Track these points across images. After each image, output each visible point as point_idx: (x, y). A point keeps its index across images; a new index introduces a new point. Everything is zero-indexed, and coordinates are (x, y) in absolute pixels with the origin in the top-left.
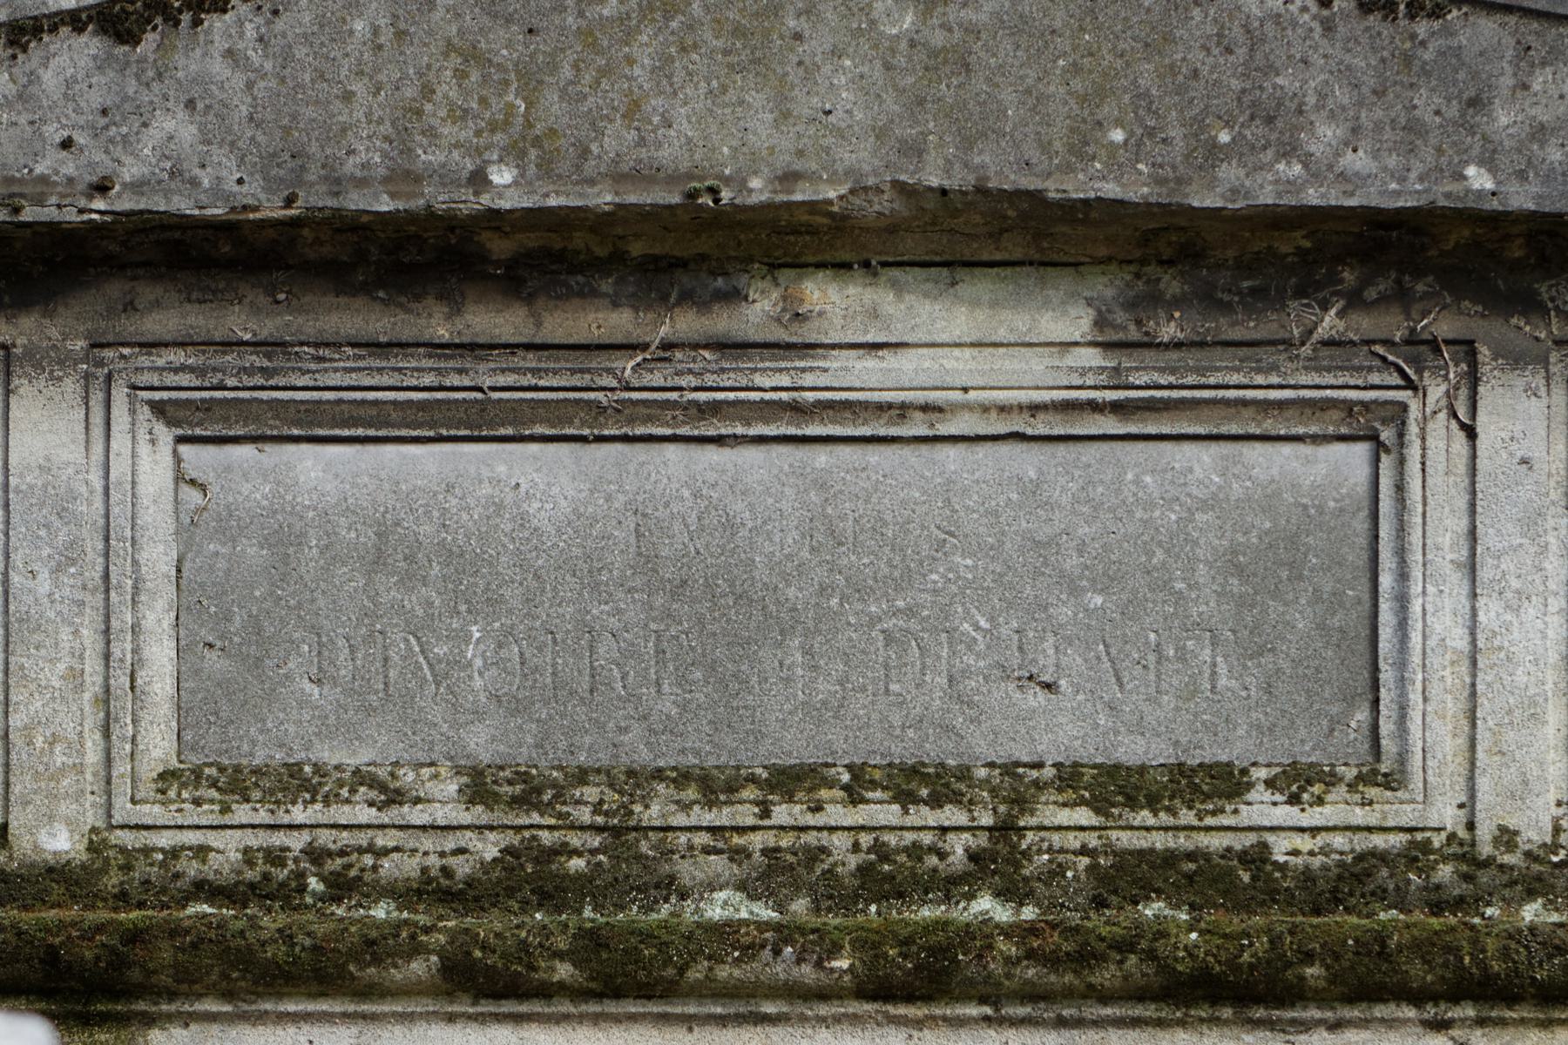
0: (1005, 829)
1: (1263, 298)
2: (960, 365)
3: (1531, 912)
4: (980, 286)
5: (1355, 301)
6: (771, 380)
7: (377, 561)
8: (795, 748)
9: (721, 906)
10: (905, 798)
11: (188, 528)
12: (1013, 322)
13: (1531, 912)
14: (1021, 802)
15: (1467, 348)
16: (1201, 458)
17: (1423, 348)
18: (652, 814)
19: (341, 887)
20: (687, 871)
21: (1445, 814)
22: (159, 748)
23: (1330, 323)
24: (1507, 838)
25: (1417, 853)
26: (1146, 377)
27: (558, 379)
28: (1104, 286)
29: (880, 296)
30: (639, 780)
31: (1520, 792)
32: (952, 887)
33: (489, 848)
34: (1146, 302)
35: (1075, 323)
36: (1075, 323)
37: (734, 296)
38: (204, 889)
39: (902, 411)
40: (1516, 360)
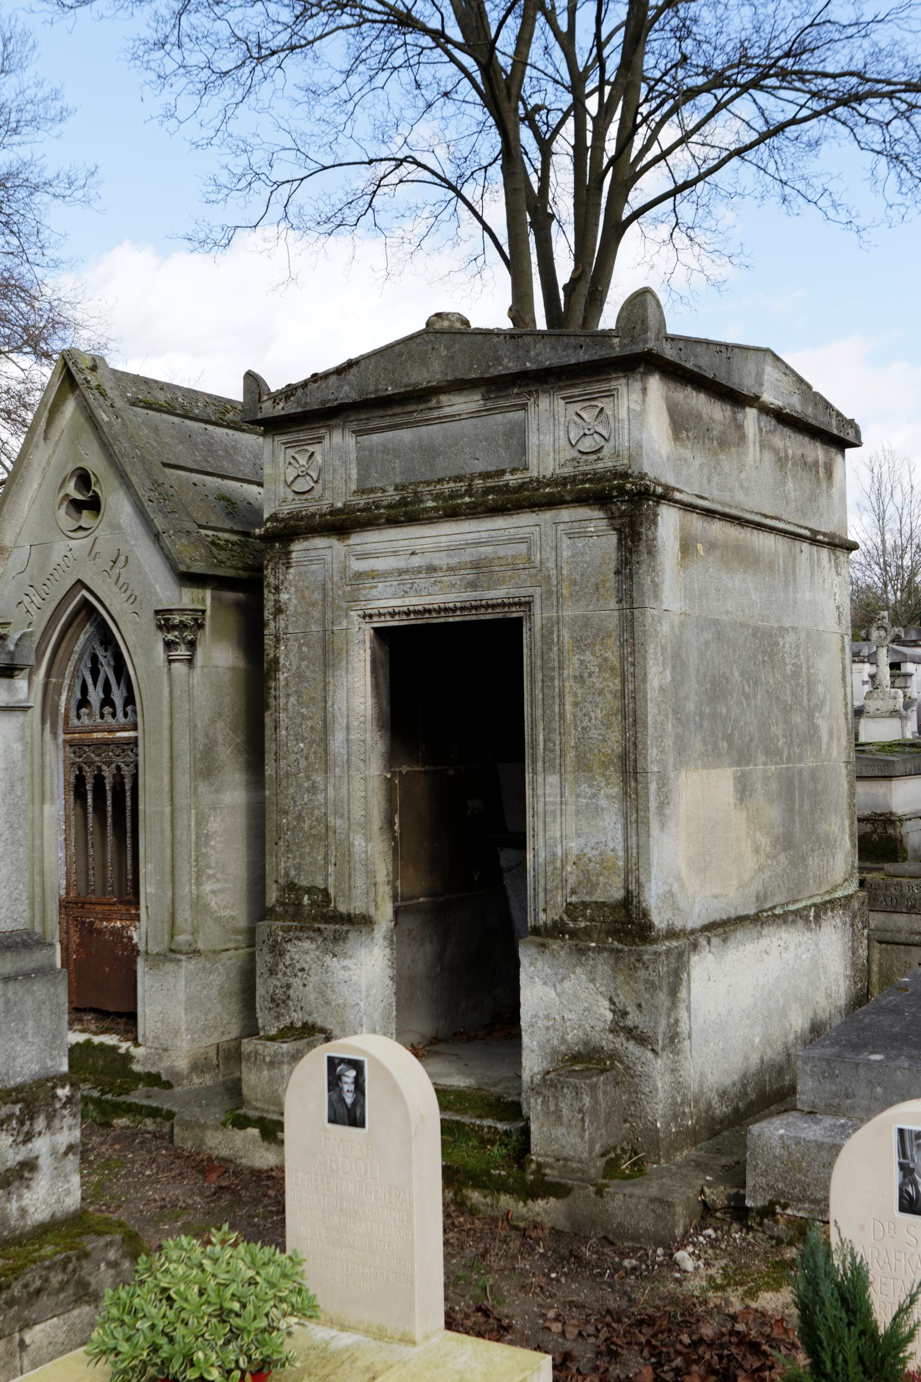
0: (470, 485)
1: (506, 388)
2: (462, 406)
3: (547, 490)
4: (465, 393)
5: (520, 386)
6: (435, 414)
7: (384, 452)
8: (441, 475)
9: (430, 504)
10: (455, 482)
11: (358, 451)
12: (470, 398)
13: (547, 490)
14: (472, 480)
15: (537, 391)
16: (499, 417)
17: (530, 393)
18: (419, 489)
19: (377, 507)
20: (424, 498)
21: (535, 474)
22: (354, 487)
23: (516, 391)
24: (544, 477)
25: (531, 482)
26: (490, 405)
27: (405, 419)
28: (483, 390)
29: (452, 397)
30: (418, 484)
31: (546, 469)
32: (462, 496)
33: (397, 498)
34: (489, 392)
35: (478, 397)
36: (479, 397)
37: (430, 400)
38: (359, 510)
39: (454, 416)
40: (544, 392)
